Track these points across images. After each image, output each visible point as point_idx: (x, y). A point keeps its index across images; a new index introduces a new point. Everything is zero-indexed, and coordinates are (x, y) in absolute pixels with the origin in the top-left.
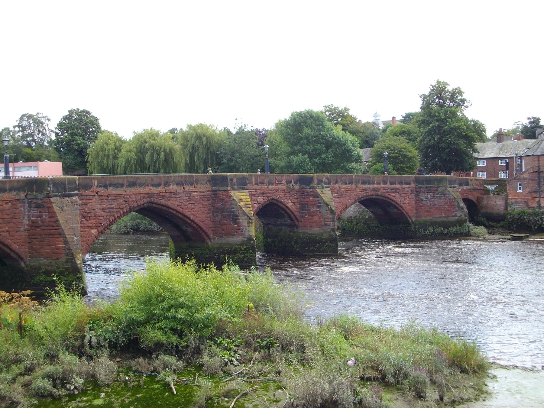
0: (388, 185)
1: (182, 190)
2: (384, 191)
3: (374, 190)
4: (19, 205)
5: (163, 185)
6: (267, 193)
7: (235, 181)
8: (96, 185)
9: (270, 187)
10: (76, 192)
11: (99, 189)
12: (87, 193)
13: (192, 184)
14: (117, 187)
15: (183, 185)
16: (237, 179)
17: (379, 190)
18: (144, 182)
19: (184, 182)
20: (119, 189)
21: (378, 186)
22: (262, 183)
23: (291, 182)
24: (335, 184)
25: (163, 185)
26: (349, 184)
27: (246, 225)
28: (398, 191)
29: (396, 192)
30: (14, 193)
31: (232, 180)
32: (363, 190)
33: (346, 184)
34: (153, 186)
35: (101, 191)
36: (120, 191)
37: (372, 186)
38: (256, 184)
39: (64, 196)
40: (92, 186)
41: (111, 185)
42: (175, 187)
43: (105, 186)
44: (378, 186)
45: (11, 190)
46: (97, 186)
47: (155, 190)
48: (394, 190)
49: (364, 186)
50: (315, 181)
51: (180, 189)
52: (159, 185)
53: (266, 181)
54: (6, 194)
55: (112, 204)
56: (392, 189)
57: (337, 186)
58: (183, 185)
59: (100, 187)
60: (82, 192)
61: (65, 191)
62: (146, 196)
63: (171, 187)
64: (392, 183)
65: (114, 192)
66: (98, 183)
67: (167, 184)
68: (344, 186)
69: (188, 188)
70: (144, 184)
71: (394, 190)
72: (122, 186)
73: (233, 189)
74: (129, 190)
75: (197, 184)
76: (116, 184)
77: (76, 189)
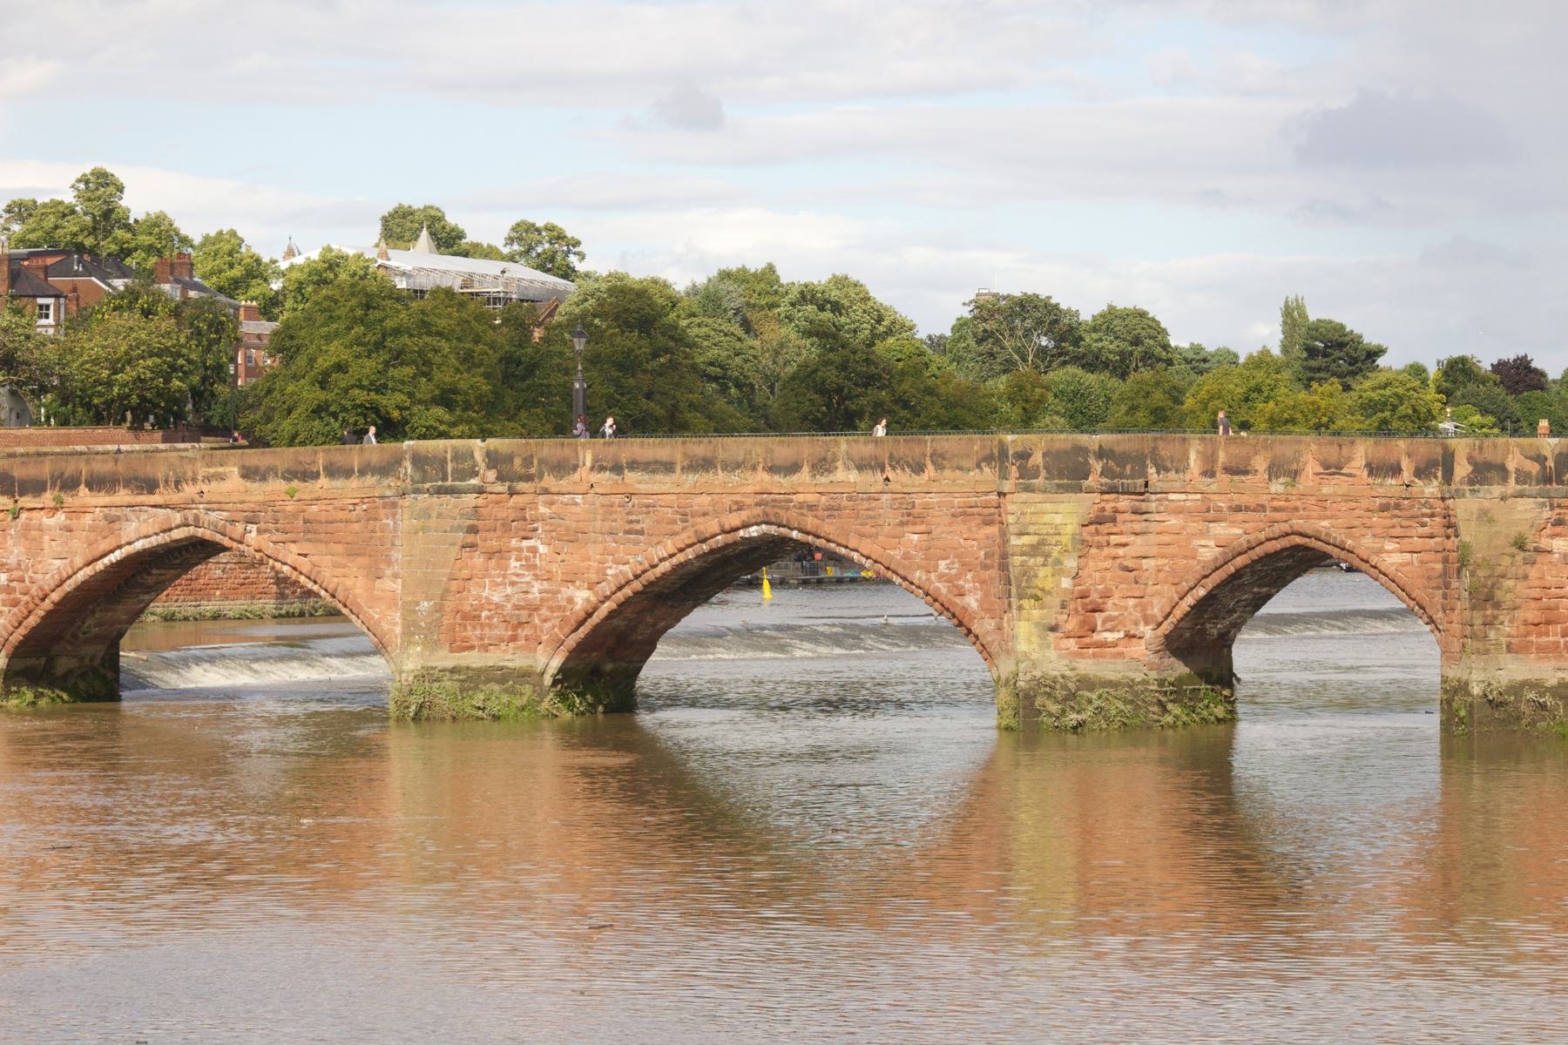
1: (880, 486)
4: (382, 512)
5: (806, 469)
6: (1262, 508)
7: (1037, 459)
9: (1277, 487)
10: (474, 481)
11: (595, 477)
12: (564, 484)
13: (919, 469)
14: (653, 472)
15: (883, 471)
16: (1044, 455)
18: (741, 459)
20: (659, 477)
23: (1396, 470)
25: (806, 469)
30: (370, 480)
31: (1024, 456)
34: (772, 469)
38: (1209, 473)
39: (440, 491)
40: (575, 468)
41: (633, 465)
42: (854, 476)
43: (617, 469)
45: (362, 473)
46: (592, 469)
47: (782, 483)
50: (1462, 469)
51: (873, 480)
52: (794, 468)
54: (354, 483)
58: (883, 471)
59: (602, 469)
60: (549, 481)
61: (444, 479)
63: (840, 475)
65: (642, 487)
66: (595, 460)
67: (822, 465)
69: (901, 478)
70: (738, 465)
72: (668, 467)
74: (692, 478)
75: (939, 467)
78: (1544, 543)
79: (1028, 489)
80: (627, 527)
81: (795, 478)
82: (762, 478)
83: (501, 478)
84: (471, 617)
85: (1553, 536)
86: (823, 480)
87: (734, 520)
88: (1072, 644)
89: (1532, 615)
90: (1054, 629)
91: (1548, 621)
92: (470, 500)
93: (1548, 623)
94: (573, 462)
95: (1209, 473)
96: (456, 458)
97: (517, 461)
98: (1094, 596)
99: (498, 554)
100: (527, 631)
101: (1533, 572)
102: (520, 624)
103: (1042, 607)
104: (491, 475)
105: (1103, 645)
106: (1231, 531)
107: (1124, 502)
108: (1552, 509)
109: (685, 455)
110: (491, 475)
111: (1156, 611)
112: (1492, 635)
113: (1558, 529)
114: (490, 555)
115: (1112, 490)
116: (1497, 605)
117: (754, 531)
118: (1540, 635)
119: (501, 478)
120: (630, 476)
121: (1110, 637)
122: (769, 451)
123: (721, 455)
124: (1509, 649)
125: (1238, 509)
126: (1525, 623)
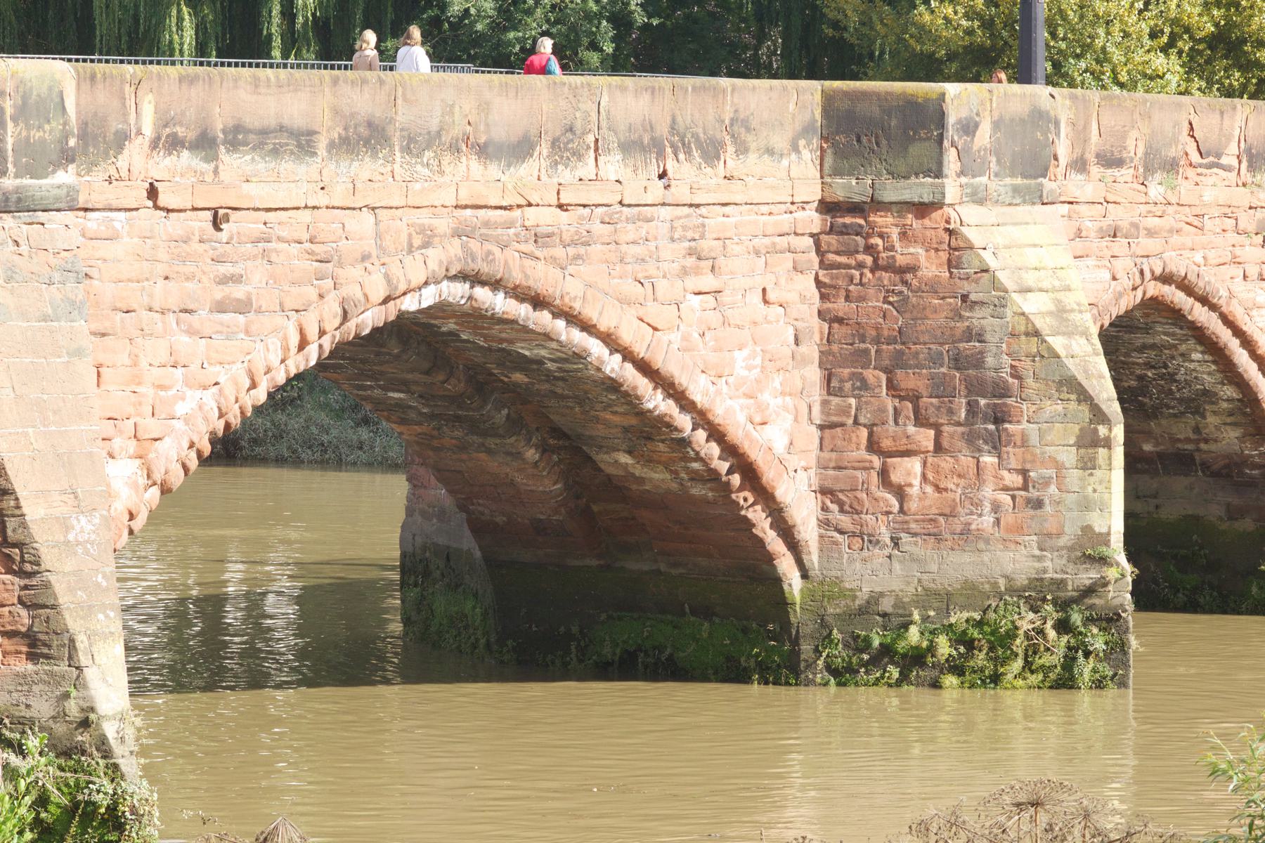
7: (984, 136)
8: (148, 130)
11: (163, 166)
14: (276, 152)
15: (661, 155)
16: (996, 125)
18: (434, 125)
19: (663, 130)
20: (287, 166)
22: (1111, 161)
27: (1068, 456)
31: (969, 128)
34: (484, 151)
35: (180, 173)
36: (289, 181)
38: (1080, 165)
40: (122, 139)
41: (237, 137)
42: (613, 165)
43: (205, 144)
46: (154, 145)
51: (639, 183)
52: (521, 149)
53: (1135, 146)
55: (236, 279)
59: (174, 144)
62: (443, 224)
65: (259, 193)
66: (164, 121)
70: (432, 140)
73: (979, 198)
75: (742, 149)
76: (264, 132)
77: (67, 157)
80: (219, 293)
81: (528, 170)
86: (565, 175)
94: (115, 125)
96: (22, 113)
109: (336, 111)
120: (233, 164)
122: (484, 107)
123: (403, 116)
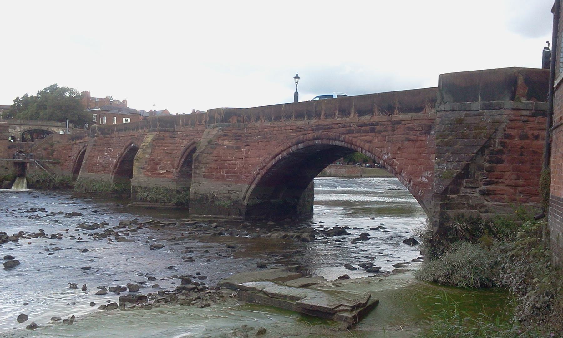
0: (353, 118)
2: (343, 130)
3: (318, 128)
9: (191, 129)
17: (329, 128)
21: (329, 121)
24: (256, 121)
26: (276, 119)
28: (378, 128)
29: (373, 130)
32: (299, 129)
33: (270, 120)
37: (314, 122)
44: (329, 121)
48: (368, 128)
49: (300, 123)
56: (361, 126)
57: (258, 124)
64: (361, 113)
68: (268, 124)
71: (368, 128)
78: (220, 142)
79: (149, 131)
82: (132, 133)
83: (102, 134)
84: (94, 165)
85: (224, 140)
87: (129, 142)
88: (149, 173)
89: (213, 166)
90: (142, 169)
91: (221, 168)
92: (95, 138)
93: (220, 169)
95: (183, 126)
97: (106, 130)
98: (157, 160)
99: (102, 151)
100: (108, 169)
101: (215, 152)
102: (106, 167)
103: (139, 162)
104: (99, 133)
105: (160, 174)
106: (185, 142)
107: (167, 134)
108: (223, 130)
110: (99, 133)
111: (176, 165)
112: (197, 171)
113: (225, 138)
114: (99, 151)
115: (162, 131)
116: (200, 162)
117: (132, 145)
118: (217, 172)
119: (102, 134)
121: (162, 172)
124: (204, 176)
125: (187, 136)
126: (211, 168)
